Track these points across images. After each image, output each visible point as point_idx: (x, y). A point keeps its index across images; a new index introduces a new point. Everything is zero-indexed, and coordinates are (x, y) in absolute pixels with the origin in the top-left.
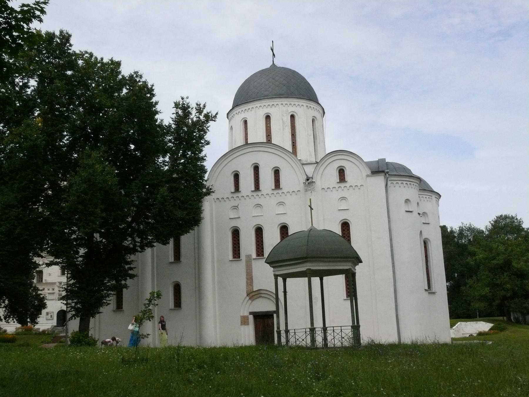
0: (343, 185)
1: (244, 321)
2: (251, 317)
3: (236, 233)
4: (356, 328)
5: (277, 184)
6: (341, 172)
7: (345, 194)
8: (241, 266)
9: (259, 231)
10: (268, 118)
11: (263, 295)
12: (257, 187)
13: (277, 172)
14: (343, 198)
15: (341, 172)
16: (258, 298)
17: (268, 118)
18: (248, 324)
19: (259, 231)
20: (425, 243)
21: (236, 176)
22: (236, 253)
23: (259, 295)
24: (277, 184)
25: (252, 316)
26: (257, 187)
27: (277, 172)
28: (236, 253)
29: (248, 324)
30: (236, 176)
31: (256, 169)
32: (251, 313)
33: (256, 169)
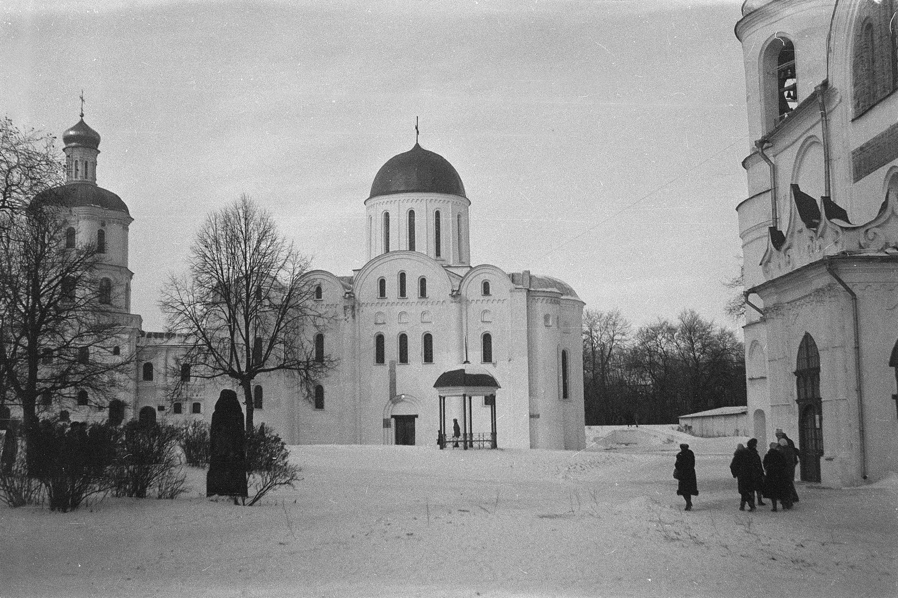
0: (487, 298)
1: (386, 424)
2: (393, 420)
3: (380, 339)
4: (494, 434)
5: (423, 293)
8: (383, 371)
9: (403, 338)
10: (412, 213)
12: (403, 293)
13: (423, 282)
17: (412, 213)
18: (390, 427)
19: (403, 338)
20: (564, 354)
21: (382, 282)
22: (380, 358)
24: (423, 293)
26: (403, 293)
27: (423, 282)
28: (380, 358)
29: (390, 427)
30: (382, 282)
31: (403, 276)
32: (392, 416)
33: (403, 276)
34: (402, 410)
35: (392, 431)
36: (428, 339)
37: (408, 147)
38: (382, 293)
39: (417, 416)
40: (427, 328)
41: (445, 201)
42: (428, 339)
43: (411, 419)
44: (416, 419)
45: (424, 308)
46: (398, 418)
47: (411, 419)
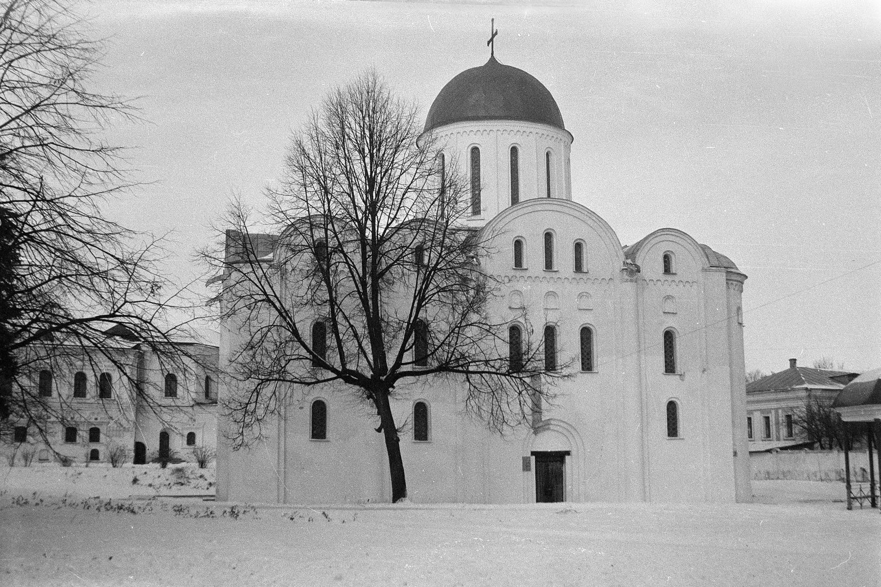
6: (667, 259)
7: (671, 290)
11: (551, 427)
12: (549, 265)
13: (578, 247)
14: (668, 297)
15: (667, 259)
16: (544, 430)
18: (530, 470)
23: (547, 427)
25: (534, 457)
27: (578, 247)
29: (530, 470)
31: (548, 236)
32: (533, 453)
33: (548, 236)
34: (549, 443)
35: (531, 477)
36: (586, 334)
37: (481, 61)
38: (518, 262)
39: (568, 453)
40: (587, 319)
41: (553, 137)
42: (586, 334)
43: (560, 457)
44: (567, 457)
45: (582, 287)
46: (541, 457)
47: (560, 457)
